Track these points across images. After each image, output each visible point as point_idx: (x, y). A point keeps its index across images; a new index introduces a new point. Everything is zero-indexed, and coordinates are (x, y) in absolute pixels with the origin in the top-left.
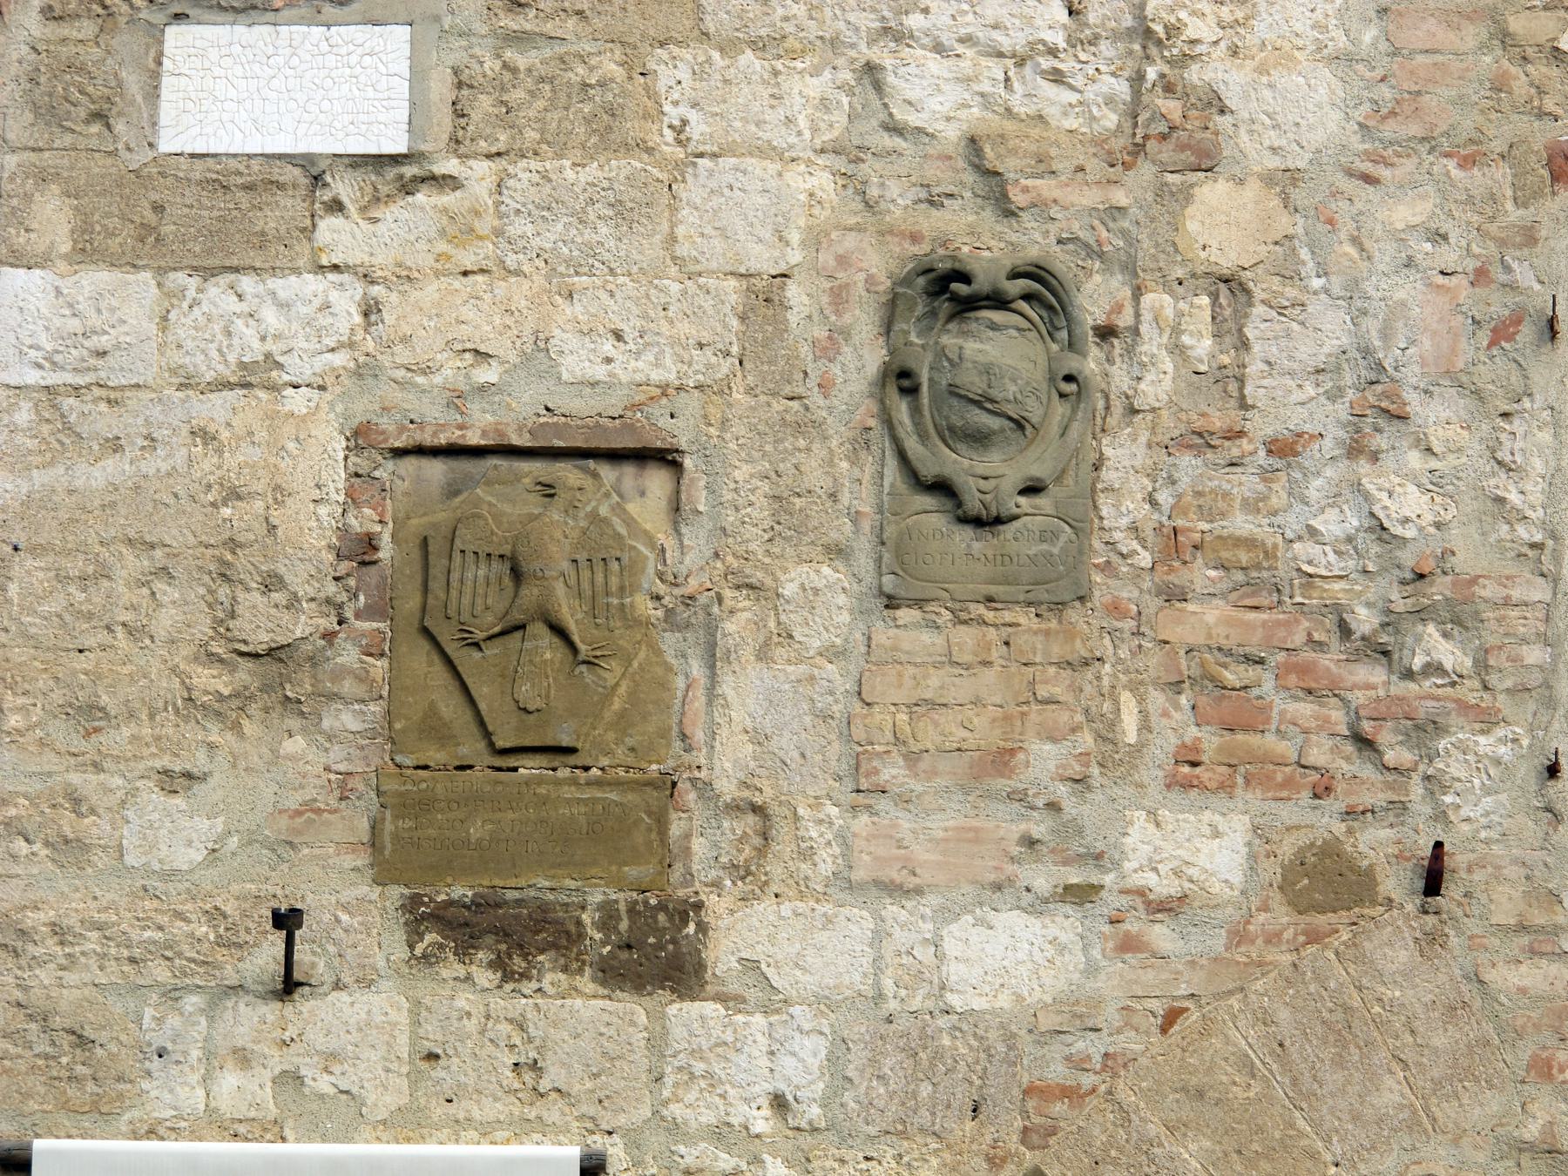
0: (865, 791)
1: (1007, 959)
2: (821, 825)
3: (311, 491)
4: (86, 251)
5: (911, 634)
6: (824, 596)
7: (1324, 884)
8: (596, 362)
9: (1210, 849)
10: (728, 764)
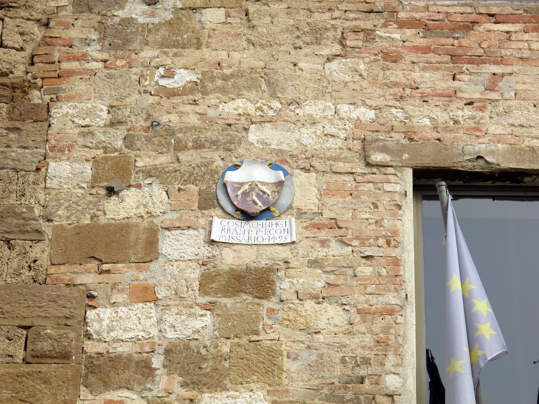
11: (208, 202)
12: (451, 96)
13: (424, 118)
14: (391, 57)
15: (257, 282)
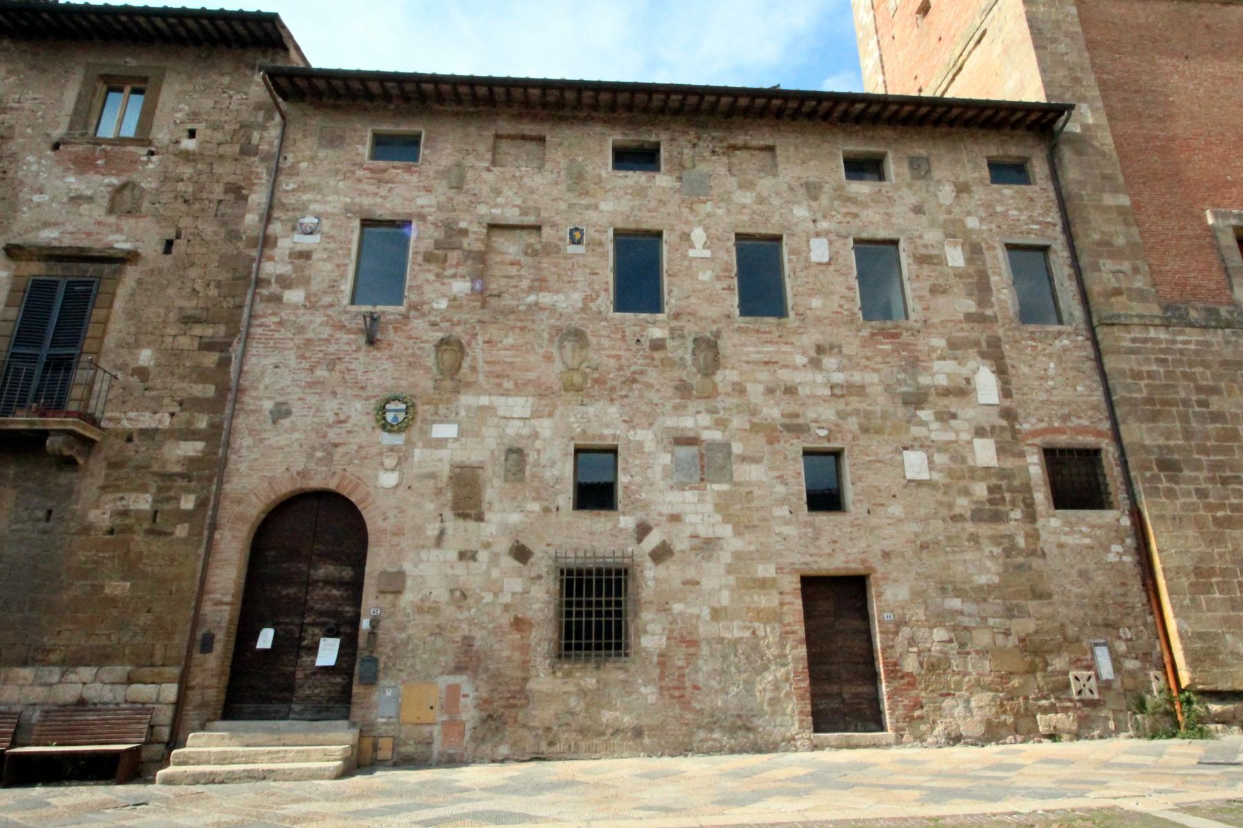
0: (501, 501)
1: (514, 518)
2: (496, 506)
3: (445, 472)
4: (424, 447)
5: (507, 486)
6: (497, 482)
7: (547, 510)
9: (536, 507)
11: (294, 229)
12: (376, 194)
13: (366, 201)
14: (360, 181)
15: (306, 255)
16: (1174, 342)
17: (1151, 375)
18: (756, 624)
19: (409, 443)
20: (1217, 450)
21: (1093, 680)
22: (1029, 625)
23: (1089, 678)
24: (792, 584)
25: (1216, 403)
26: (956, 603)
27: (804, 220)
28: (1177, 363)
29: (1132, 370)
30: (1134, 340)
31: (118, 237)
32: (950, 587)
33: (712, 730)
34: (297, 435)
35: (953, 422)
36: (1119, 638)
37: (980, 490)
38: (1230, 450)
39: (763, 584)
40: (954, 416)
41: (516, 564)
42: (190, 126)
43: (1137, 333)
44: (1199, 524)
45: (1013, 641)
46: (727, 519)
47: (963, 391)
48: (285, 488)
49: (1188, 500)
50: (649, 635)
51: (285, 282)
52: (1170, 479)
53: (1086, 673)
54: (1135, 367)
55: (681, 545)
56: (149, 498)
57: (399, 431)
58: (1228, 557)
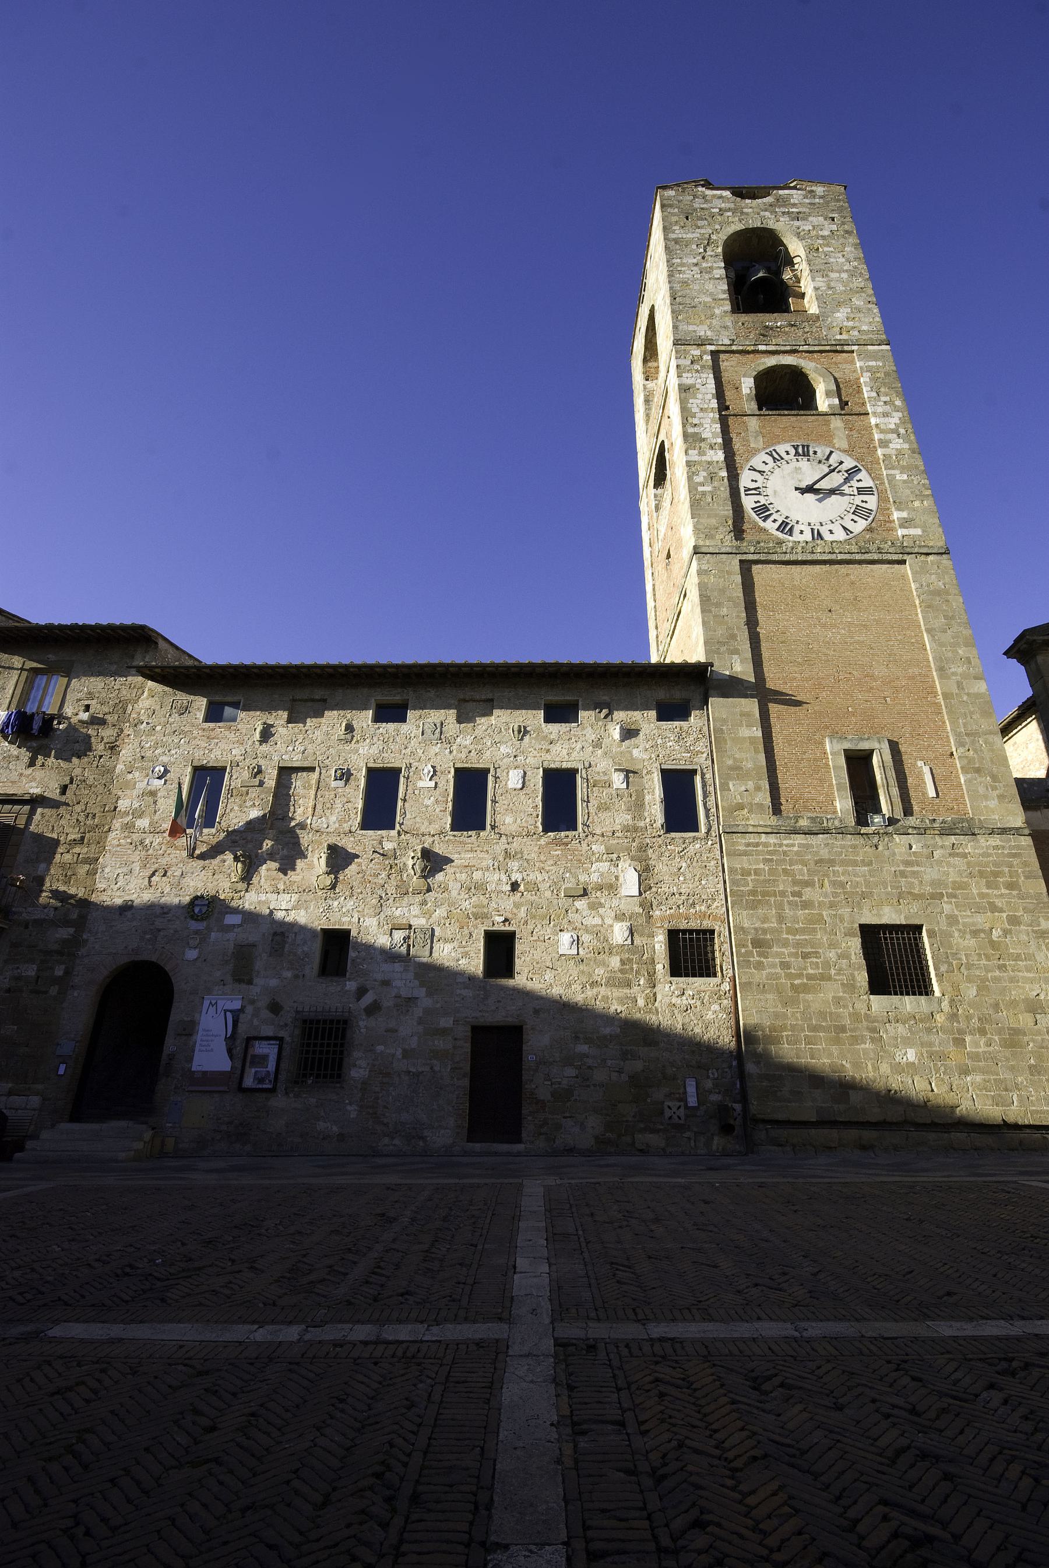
1: (274, 982)
6: (265, 956)
7: (296, 977)
8: (251, 939)
9: (289, 974)
10: (257, 968)
16: (781, 845)
17: (757, 872)
18: (435, 1062)
19: (209, 929)
20: (803, 931)
21: (682, 1110)
22: (639, 1066)
23: (679, 1107)
24: (464, 1032)
25: (808, 893)
26: (583, 1048)
27: (508, 756)
28: (779, 862)
29: (742, 869)
30: (748, 845)
31: (34, 784)
32: (581, 1036)
33: (393, 1138)
34: (135, 924)
35: (601, 911)
36: (708, 1077)
37: (615, 962)
38: (814, 930)
39: (444, 1032)
40: (601, 905)
41: (273, 1016)
42: (86, 703)
43: (752, 839)
44: (779, 990)
45: (624, 1077)
46: (422, 985)
47: (611, 887)
48: (123, 960)
49: (773, 971)
50: (358, 1069)
51: (139, 814)
52: (760, 955)
53: (678, 1104)
54: (746, 866)
55: (387, 1003)
56: (35, 967)
57: (202, 920)
58: (798, 1015)
